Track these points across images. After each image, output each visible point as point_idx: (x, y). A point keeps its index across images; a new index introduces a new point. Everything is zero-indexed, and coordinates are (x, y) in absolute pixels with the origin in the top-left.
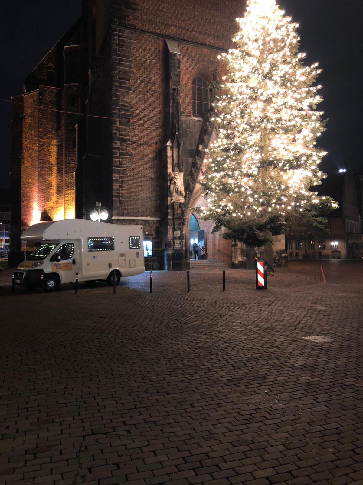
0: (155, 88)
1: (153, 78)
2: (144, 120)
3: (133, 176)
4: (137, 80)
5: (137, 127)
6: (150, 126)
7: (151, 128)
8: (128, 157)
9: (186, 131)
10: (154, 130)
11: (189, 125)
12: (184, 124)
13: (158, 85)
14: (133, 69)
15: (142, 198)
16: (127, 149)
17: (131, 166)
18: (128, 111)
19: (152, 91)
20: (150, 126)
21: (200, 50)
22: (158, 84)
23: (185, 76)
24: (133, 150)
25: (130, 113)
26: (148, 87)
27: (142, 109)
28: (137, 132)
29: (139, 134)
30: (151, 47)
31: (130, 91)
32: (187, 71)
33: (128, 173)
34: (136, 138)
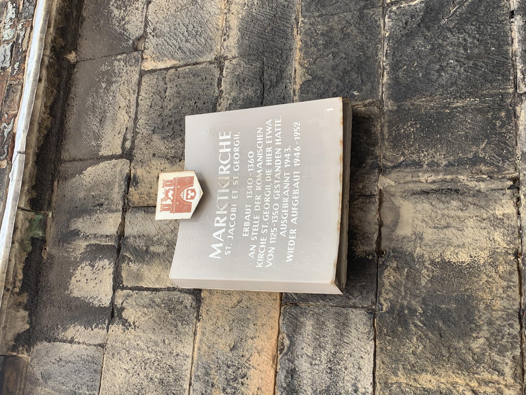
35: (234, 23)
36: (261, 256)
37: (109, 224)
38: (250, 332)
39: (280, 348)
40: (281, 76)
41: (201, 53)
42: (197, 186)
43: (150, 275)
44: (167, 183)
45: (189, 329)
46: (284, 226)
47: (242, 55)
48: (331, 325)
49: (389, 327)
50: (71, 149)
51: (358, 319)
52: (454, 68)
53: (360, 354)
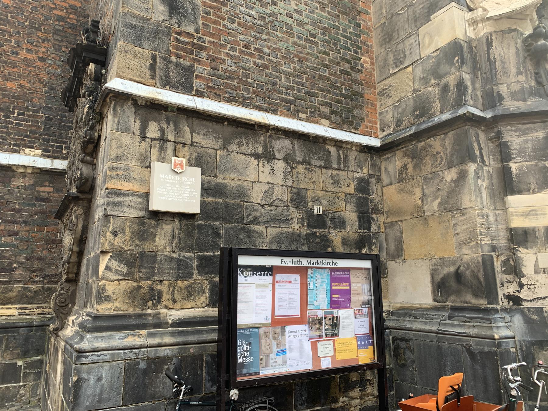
35: (226, 181)
36: (160, 189)
37: (171, 137)
38: (139, 183)
39: (134, 192)
40: (209, 195)
41: (219, 171)
42: (181, 171)
43: (155, 152)
44: (182, 161)
45: (139, 164)
46: (168, 196)
47: (216, 183)
48: (141, 206)
49: (140, 221)
50: (196, 122)
51: (142, 213)
52: (203, 239)
53: (134, 213)
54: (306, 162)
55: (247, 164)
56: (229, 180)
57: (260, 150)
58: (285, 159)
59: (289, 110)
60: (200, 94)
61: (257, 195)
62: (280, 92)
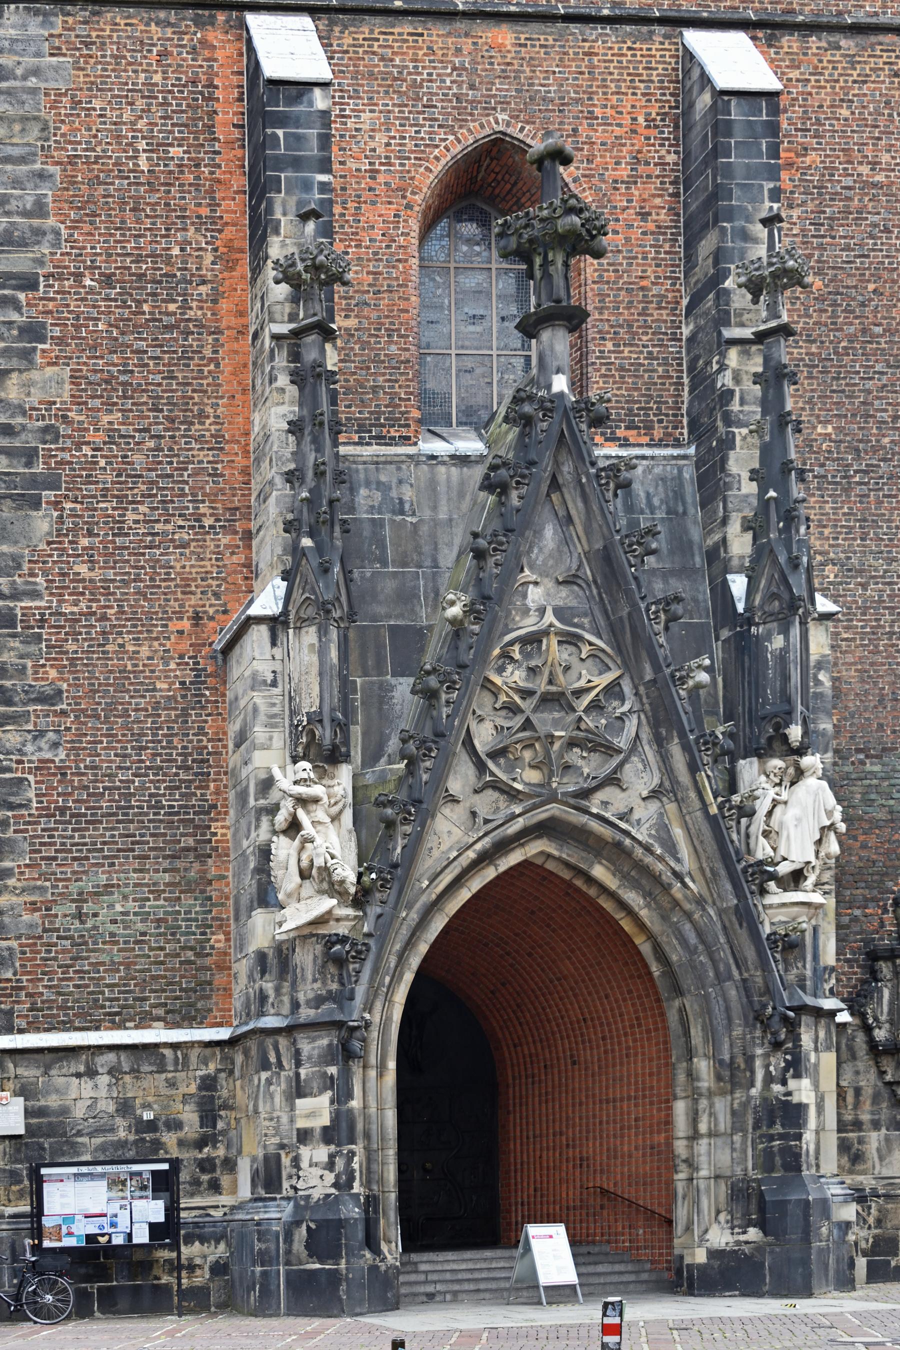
0: (185, 307)
1: (176, 251)
2: (120, 498)
3: (63, 810)
4: (78, 276)
5: (85, 542)
6: (158, 527)
7: (165, 533)
8: (31, 708)
9: (377, 524)
10: (184, 545)
11: (394, 494)
12: (363, 492)
13: (203, 289)
14: (52, 221)
15: (112, 928)
16: (24, 667)
17: (48, 755)
18: (30, 455)
19: (169, 328)
20: (158, 527)
21: (467, 45)
22: (204, 282)
23: (368, 214)
24: (60, 669)
25: (39, 468)
26: (146, 308)
27: (112, 436)
28: (83, 569)
29: (97, 575)
30: (157, 78)
31: (40, 346)
32: (381, 178)
33: (31, 794)
34: (76, 603)
40: (33, 1117)
50: (18, 1057)
52: (30, 1153)
54: (135, 1072)
55: (68, 1085)
56: (52, 1102)
57: (82, 1069)
58: (109, 1073)
59: (113, 1022)
60: (21, 1031)
61: (79, 1111)
62: (103, 1007)
